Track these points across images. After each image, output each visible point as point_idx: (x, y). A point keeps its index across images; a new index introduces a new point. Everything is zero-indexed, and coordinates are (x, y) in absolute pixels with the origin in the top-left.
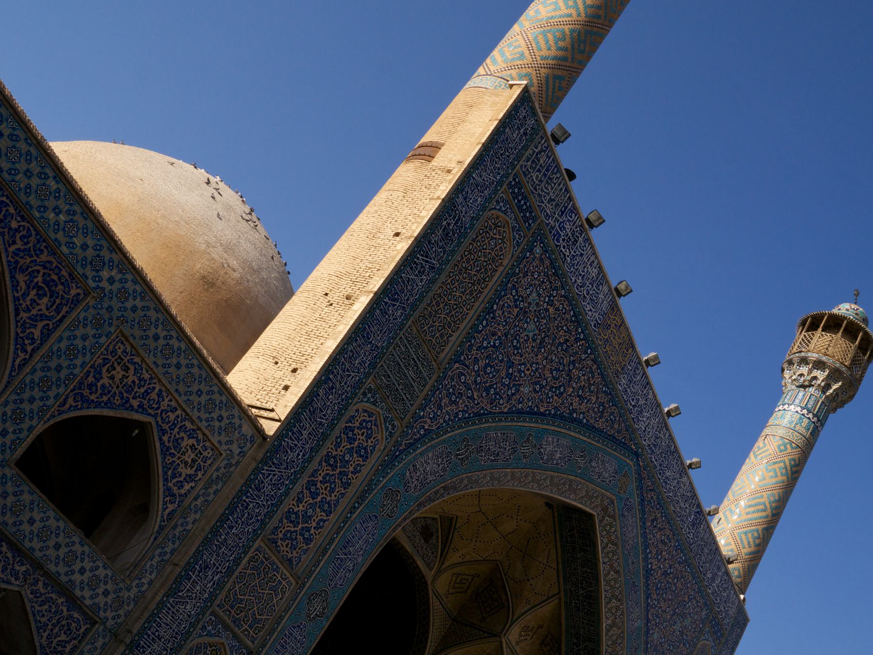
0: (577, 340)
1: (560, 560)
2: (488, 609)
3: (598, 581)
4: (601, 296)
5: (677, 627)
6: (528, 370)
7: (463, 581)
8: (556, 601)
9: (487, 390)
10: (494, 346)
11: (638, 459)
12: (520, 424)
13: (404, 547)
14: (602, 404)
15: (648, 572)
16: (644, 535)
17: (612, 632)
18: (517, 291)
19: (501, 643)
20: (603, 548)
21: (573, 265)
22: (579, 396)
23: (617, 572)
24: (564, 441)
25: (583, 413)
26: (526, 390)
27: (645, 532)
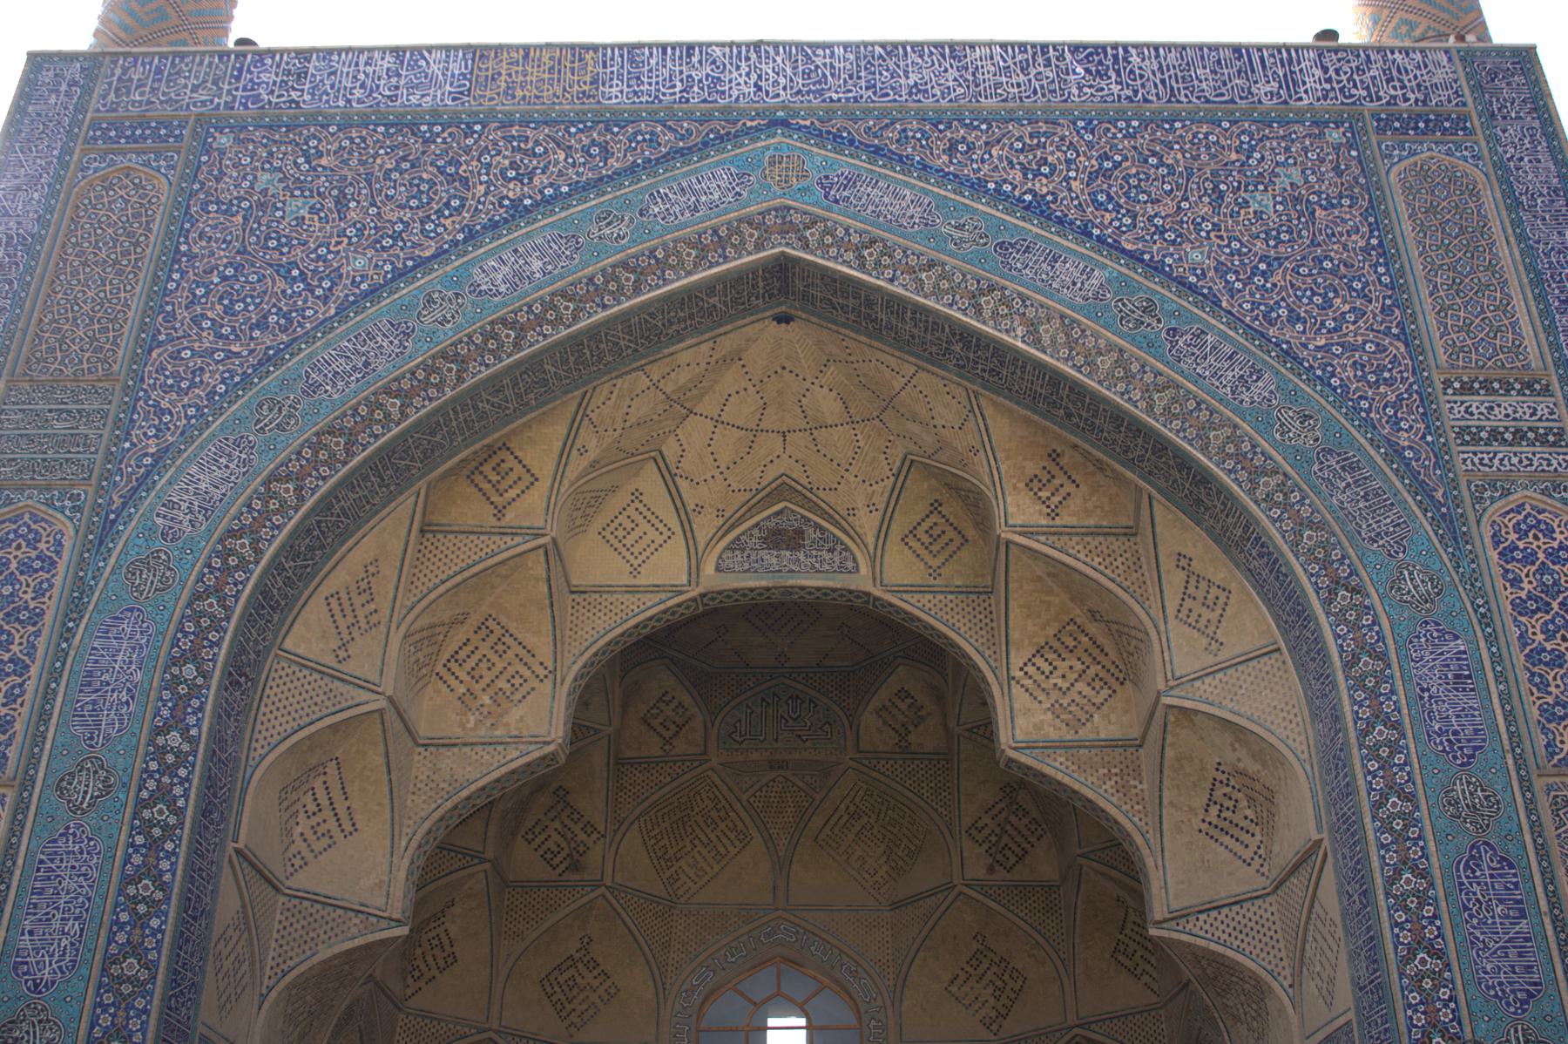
3: (927, 311)
6: (338, 243)
10: (225, 278)
15: (1039, 209)
16: (944, 176)
17: (1046, 340)
20: (862, 267)
22: (511, 179)
23: (931, 265)
25: (551, 185)
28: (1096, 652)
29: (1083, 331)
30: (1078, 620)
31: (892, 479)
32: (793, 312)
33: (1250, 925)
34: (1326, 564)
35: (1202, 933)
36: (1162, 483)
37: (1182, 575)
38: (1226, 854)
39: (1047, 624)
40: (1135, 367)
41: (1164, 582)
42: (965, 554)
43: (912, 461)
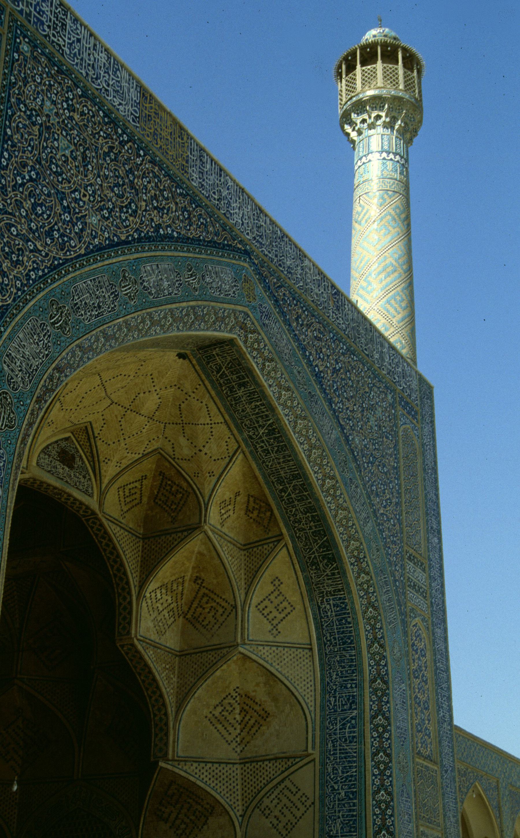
0: (122, 144)
1: (222, 410)
2: (174, 507)
3: (272, 409)
4: (124, 84)
5: (372, 422)
6: (85, 196)
7: (133, 491)
8: (241, 457)
9: (49, 234)
10: (31, 180)
11: (250, 258)
12: (107, 262)
13: (49, 485)
14: (184, 209)
18: (25, 105)
19: (205, 533)
21: (75, 54)
22: (155, 208)
23: (288, 389)
24: (164, 266)
26: (94, 220)
27: (295, 335)
28: (179, 596)
29: (328, 463)
30: (186, 578)
31: (141, 455)
32: (191, 357)
33: (222, 777)
34: (373, 628)
35: (194, 774)
36: (300, 545)
37: (272, 588)
38: (217, 735)
39: (174, 574)
40: (338, 493)
41: (258, 586)
42: (136, 509)
43: (159, 453)
